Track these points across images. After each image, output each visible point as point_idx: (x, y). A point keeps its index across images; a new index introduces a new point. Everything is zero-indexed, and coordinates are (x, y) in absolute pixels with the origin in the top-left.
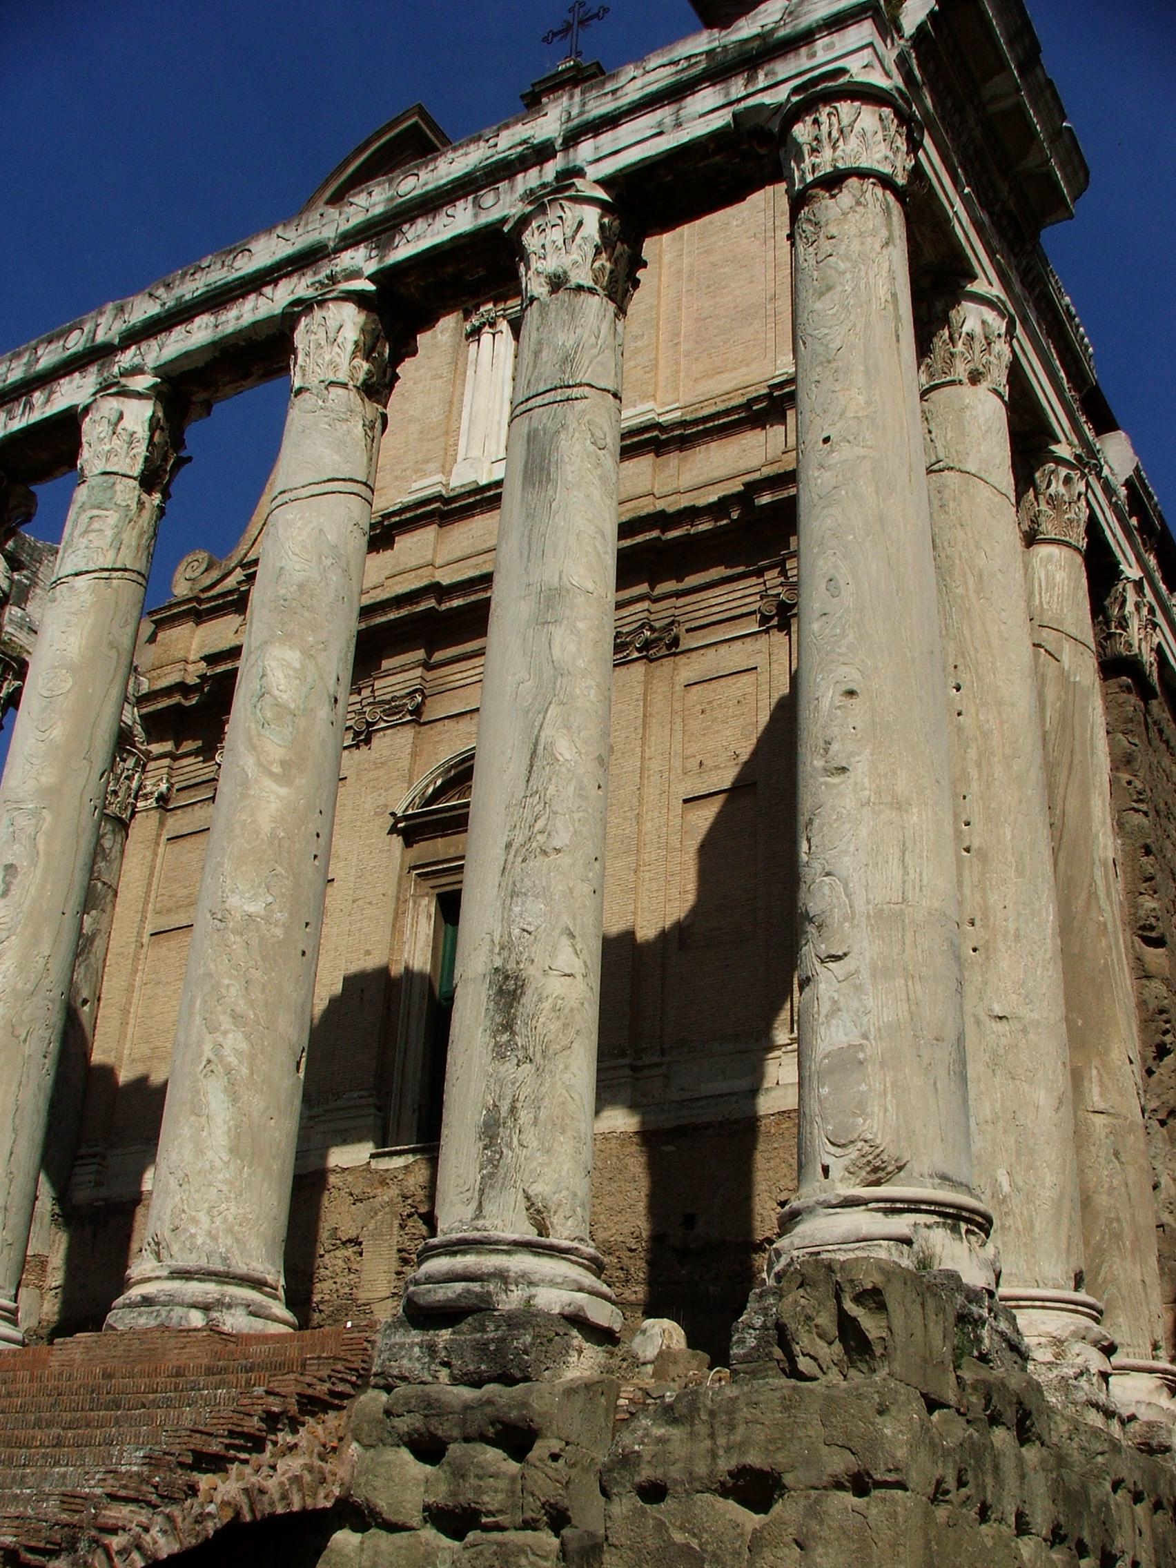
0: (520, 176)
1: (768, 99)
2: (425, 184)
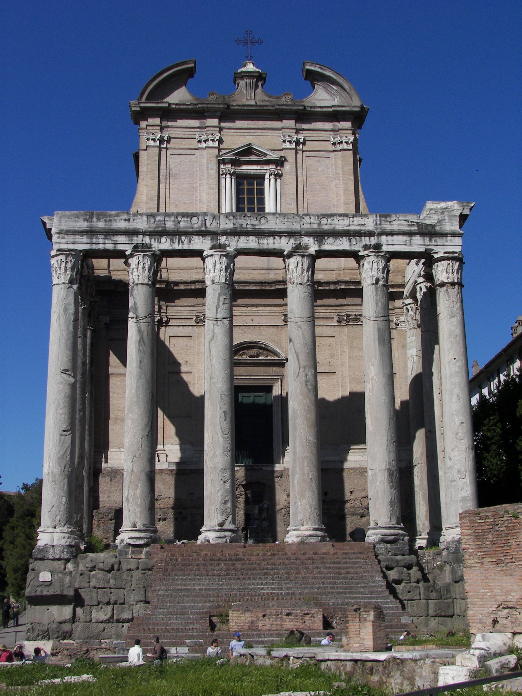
0: (363, 238)
1: (436, 249)
2: (331, 224)
